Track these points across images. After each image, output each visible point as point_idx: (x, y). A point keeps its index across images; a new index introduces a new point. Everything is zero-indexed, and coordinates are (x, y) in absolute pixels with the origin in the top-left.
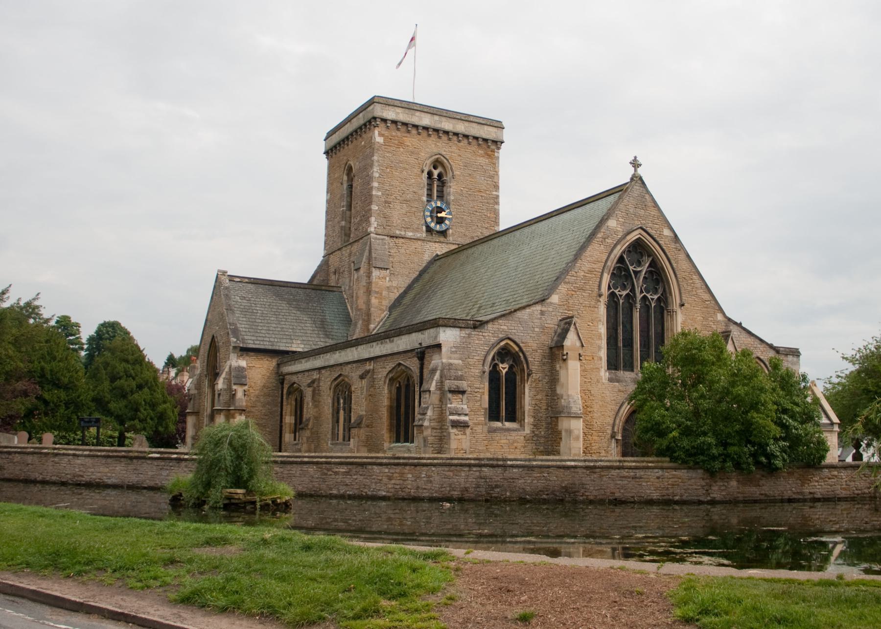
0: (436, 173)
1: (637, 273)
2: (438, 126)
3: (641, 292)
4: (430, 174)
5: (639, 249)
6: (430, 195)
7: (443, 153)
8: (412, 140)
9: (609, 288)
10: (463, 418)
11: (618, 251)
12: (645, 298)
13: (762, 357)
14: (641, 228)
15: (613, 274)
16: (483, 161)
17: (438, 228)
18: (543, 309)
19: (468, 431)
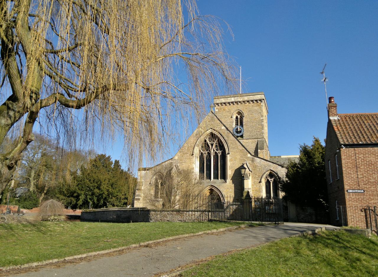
0: (239, 117)
1: (212, 145)
2: (237, 100)
3: (214, 151)
4: (237, 118)
5: (213, 136)
6: (237, 124)
7: (240, 109)
8: (227, 108)
9: (200, 150)
10: (139, 197)
11: (202, 138)
12: (216, 153)
13: (273, 170)
14: (211, 129)
15: (202, 147)
16: (256, 108)
17: (239, 135)
18: (172, 162)
19: (139, 201)
